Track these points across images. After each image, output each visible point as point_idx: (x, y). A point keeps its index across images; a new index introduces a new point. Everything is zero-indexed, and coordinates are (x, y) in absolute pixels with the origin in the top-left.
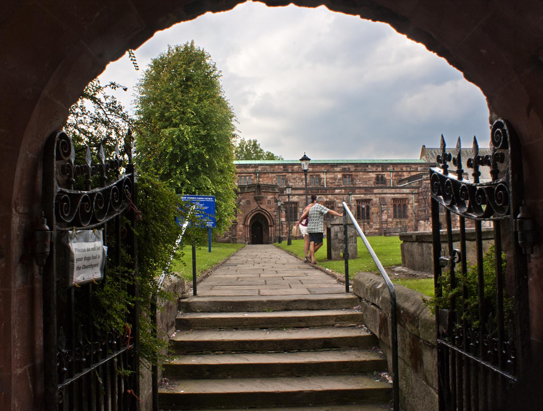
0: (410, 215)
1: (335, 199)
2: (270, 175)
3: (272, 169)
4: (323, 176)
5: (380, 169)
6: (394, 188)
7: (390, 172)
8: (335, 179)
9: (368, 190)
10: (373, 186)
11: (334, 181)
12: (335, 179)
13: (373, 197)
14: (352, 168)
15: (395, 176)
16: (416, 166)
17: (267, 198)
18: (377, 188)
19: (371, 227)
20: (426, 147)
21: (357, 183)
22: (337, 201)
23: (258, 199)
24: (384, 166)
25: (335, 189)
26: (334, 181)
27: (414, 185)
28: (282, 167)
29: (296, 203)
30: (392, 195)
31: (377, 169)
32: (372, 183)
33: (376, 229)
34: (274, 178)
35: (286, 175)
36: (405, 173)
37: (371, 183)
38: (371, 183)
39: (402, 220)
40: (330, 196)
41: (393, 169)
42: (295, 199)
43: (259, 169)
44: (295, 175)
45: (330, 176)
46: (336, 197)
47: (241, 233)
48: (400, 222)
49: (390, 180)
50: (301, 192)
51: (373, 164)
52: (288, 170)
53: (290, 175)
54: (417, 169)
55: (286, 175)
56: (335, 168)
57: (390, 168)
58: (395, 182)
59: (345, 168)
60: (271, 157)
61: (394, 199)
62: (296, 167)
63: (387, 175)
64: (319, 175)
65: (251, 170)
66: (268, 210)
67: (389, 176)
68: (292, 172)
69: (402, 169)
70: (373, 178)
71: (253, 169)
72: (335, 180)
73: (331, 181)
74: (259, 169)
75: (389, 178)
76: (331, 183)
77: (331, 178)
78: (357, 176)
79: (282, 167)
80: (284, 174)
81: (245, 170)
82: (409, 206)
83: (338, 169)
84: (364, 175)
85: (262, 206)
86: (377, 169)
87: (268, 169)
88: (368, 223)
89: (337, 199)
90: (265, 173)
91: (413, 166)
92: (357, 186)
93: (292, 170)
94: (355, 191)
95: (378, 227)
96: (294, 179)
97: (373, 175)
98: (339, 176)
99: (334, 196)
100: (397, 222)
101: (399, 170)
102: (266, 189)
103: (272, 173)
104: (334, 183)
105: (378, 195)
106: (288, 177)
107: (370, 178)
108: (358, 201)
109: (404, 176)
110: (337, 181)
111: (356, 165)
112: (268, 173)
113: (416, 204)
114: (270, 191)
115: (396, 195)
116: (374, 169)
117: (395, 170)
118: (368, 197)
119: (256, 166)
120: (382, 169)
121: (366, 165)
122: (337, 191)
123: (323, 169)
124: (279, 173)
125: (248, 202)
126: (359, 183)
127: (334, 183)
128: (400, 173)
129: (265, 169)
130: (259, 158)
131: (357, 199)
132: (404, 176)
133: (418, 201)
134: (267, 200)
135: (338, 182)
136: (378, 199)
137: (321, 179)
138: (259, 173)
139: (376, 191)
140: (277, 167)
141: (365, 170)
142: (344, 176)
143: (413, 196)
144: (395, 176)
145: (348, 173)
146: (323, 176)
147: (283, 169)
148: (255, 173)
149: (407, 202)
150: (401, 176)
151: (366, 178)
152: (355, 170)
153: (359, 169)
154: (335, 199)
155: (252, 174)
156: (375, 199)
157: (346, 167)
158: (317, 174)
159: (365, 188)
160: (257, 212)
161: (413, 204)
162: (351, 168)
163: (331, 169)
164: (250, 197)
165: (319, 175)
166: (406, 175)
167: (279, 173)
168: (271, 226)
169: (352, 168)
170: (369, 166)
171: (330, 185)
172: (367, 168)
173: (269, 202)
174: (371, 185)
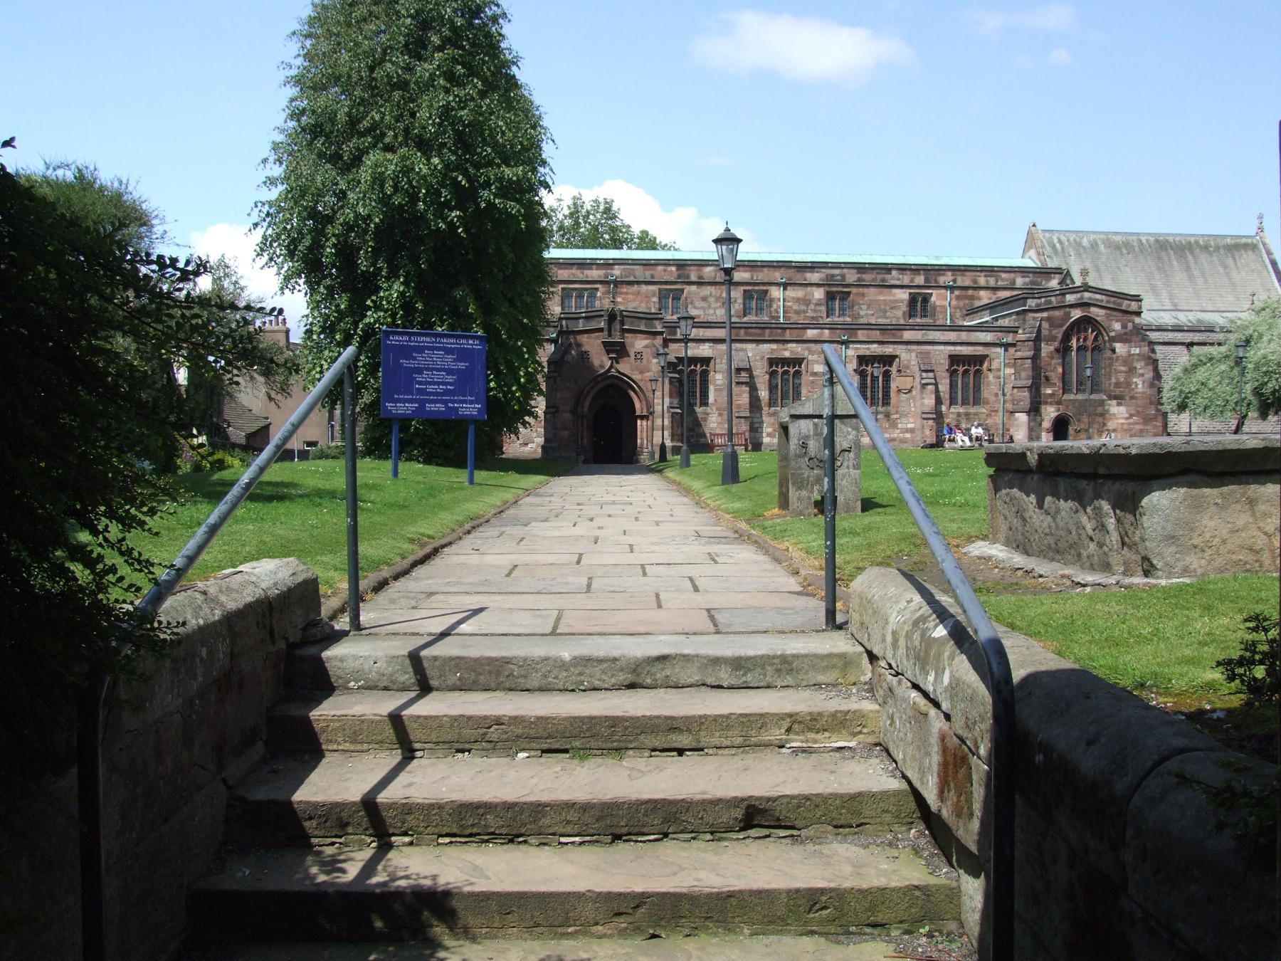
0: (992, 398)
1: (806, 353)
2: (644, 288)
3: (648, 273)
4: (776, 293)
5: (920, 280)
6: (954, 328)
7: (946, 288)
8: (806, 301)
9: (890, 331)
10: (902, 322)
11: (803, 307)
12: (806, 301)
13: (899, 350)
14: (851, 277)
15: (958, 298)
16: (1012, 275)
17: (633, 345)
18: (913, 328)
19: (894, 425)
20: (1039, 227)
21: (862, 313)
24: (931, 271)
25: (805, 327)
26: (803, 307)
27: (1005, 322)
28: (674, 269)
29: (706, 361)
30: (952, 348)
31: (912, 281)
32: (899, 313)
33: (907, 431)
34: (654, 295)
36: (982, 293)
37: (898, 316)
38: (898, 316)
39: (972, 410)
41: (954, 281)
42: (704, 350)
43: (617, 271)
44: (707, 290)
45: (793, 293)
47: (566, 433)
48: (967, 414)
49: (944, 307)
50: (720, 333)
51: (903, 268)
52: (688, 276)
53: (694, 288)
54: (1014, 282)
55: (682, 290)
56: (808, 275)
57: (946, 279)
58: (958, 315)
59: (833, 276)
60: (647, 242)
61: (954, 359)
62: (709, 269)
63: (936, 297)
65: (595, 274)
66: (636, 377)
67: (940, 299)
68: (699, 284)
69: (975, 282)
70: (902, 301)
71: (602, 272)
72: (808, 305)
73: (796, 307)
74: (617, 271)
75: (944, 303)
76: (797, 312)
77: (798, 300)
78: (863, 295)
79: (674, 269)
81: (578, 274)
82: (991, 376)
83: (814, 277)
84: (881, 293)
85: (624, 367)
86: (912, 281)
87: (640, 273)
88: (887, 416)
91: (1004, 275)
92: (863, 321)
93: (700, 277)
94: (856, 335)
95: (909, 426)
96: (704, 299)
97: (903, 295)
98: (819, 294)
100: (959, 415)
101: (967, 283)
102: (632, 323)
104: (805, 312)
105: (915, 347)
106: (689, 293)
107: (896, 301)
108: (862, 360)
109: (979, 299)
110: (812, 307)
111: (861, 268)
112: (639, 283)
113: (1010, 371)
114: (643, 328)
115: (959, 348)
116: (906, 279)
117: (959, 283)
118: (888, 350)
119: (608, 264)
120: (926, 280)
121: (886, 268)
122: (811, 333)
123: (777, 276)
126: (866, 314)
127: (805, 312)
128: (970, 292)
129: (632, 273)
130: (617, 244)
131: (861, 353)
132: (979, 299)
133: (1014, 363)
135: (815, 311)
136: (913, 355)
137: (772, 300)
139: (908, 335)
140: (660, 268)
141: (883, 280)
142: (830, 297)
143: (1001, 351)
144: (958, 298)
145: (840, 289)
146: (776, 293)
147: (675, 274)
149: (986, 365)
150: (972, 298)
151: (885, 303)
152: (859, 280)
153: (868, 277)
154: (806, 353)
156: (907, 356)
157: (836, 272)
159: (883, 329)
160: (608, 382)
161: (999, 370)
162: (848, 276)
163: (798, 278)
165: (766, 292)
166: (985, 297)
167: (666, 283)
168: (642, 418)
169: (851, 277)
170: (894, 272)
171: (794, 318)
172: (887, 276)
174: (898, 319)
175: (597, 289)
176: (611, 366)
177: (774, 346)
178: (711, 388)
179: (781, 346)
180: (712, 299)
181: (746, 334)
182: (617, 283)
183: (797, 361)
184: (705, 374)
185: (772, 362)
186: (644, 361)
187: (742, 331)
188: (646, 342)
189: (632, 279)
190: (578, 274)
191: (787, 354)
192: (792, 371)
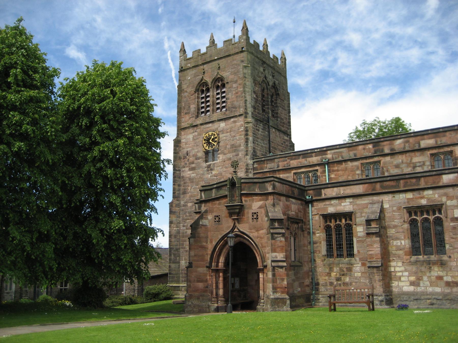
1: (444, 199)
2: (350, 164)
17: (250, 207)
22: (449, 203)
23: (237, 212)
25: (440, 173)
28: (370, 146)
29: (348, 216)
34: (358, 168)
35: (379, 162)
40: (430, 192)
42: (346, 206)
43: (329, 155)
46: (446, 195)
50: (358, 189)
52: (383, 150)
53: (388, 159)
55: (379, 162)
64: (451, 152)
65: (315, 160)
68: (393, 154)
71: (319, 158)
74: (329, 155)
79: (370, 146)
80: (376, 159)
81: (304, 162)
85: (243, 227)
89: (450, 198)
90: (340, 162)
93: (392, 149)
99: (442, 191)
103: (352, 160)
106: (385, 163)
112: (345, 161)
114: (257, 191)
122: (447, 178)
124: (366, 158)
125: (218, 219)
134: (251, 212)
138: (328, 163)
140: (361, 147)
147: (373, 151)
148: (322, 165)
155: (317, 168)
158: (449, 149)
164: (220, 208)
165: (451, 152)
167: (366, 158)
173: (255, 216)
175: (317, 170)
176: (234, 227)
177: (410, 195)
178: (355, 240)
179: (416, 194)
180: (403, 166)
181: (382, 187)
182: (329, 163)
183: (437, 208)
184: (349, 228)
185: (412, 211)
186: (259, 219)
187: (378, 186)
188: (261, 203)
189: (340, 159)
190: (304, 162)
191: (424, 202)
192: (431, 218)
